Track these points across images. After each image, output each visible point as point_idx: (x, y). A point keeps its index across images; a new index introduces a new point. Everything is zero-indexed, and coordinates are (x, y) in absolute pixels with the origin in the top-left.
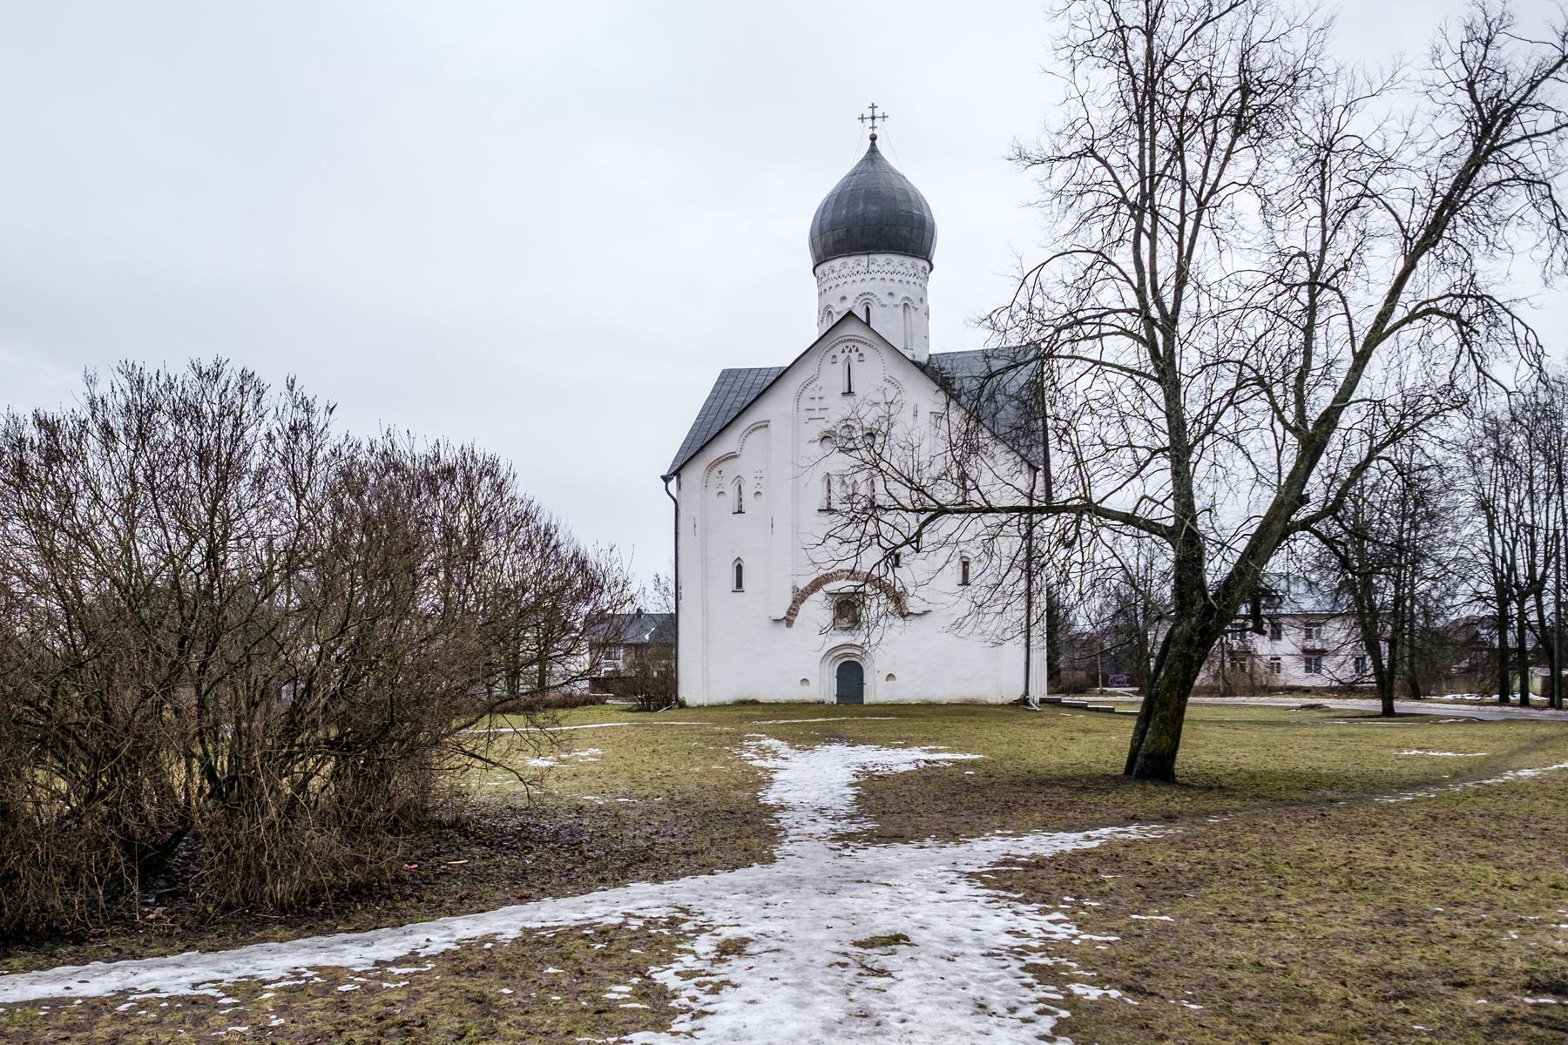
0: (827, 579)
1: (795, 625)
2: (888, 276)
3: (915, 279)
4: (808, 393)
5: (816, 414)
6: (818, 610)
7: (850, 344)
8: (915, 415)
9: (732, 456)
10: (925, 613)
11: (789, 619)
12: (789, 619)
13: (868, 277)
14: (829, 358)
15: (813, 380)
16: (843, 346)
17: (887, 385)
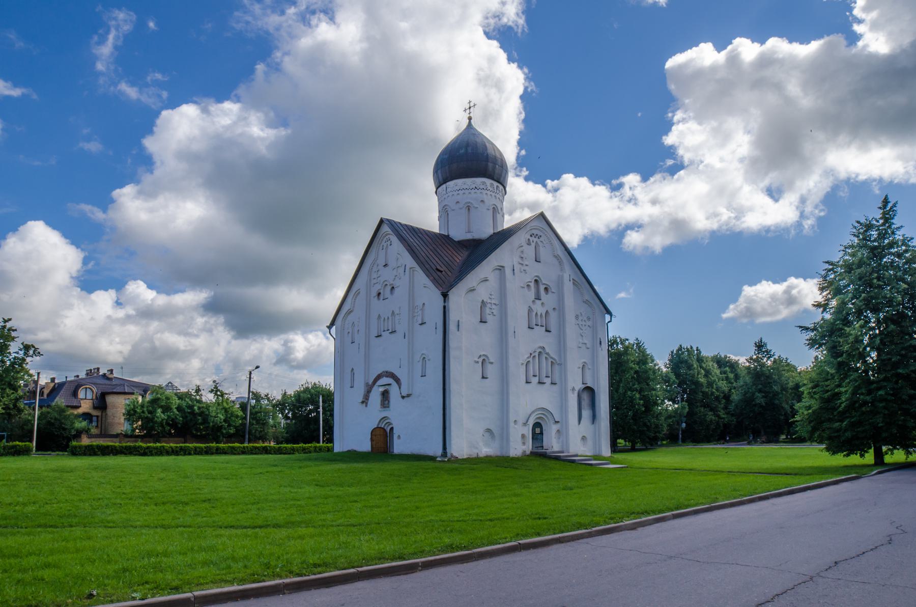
0: (379, 377)
1: (368, 406)
2: (455, 193)
3: (476, 190)
4: (375, 269)
5: (375, 281)
6: (376, 396)
7: (387, 237)
8: (405, 271)
9: (350, 312)
10: (409, 396)
11: (365, 401)
12: (365, 401)
13: (447, 195)
14: (381, 248)
15: (375, 260)
16: (385, 239)
17: (399, 256)
